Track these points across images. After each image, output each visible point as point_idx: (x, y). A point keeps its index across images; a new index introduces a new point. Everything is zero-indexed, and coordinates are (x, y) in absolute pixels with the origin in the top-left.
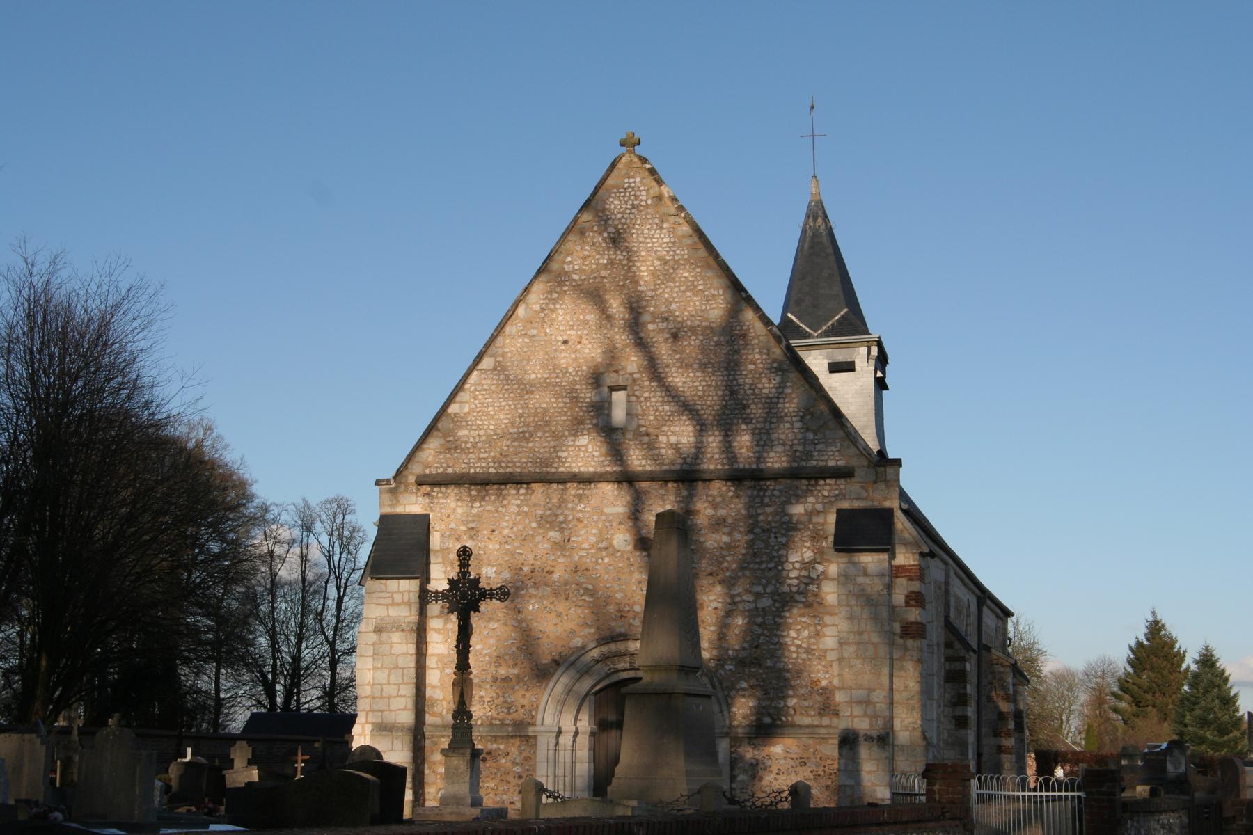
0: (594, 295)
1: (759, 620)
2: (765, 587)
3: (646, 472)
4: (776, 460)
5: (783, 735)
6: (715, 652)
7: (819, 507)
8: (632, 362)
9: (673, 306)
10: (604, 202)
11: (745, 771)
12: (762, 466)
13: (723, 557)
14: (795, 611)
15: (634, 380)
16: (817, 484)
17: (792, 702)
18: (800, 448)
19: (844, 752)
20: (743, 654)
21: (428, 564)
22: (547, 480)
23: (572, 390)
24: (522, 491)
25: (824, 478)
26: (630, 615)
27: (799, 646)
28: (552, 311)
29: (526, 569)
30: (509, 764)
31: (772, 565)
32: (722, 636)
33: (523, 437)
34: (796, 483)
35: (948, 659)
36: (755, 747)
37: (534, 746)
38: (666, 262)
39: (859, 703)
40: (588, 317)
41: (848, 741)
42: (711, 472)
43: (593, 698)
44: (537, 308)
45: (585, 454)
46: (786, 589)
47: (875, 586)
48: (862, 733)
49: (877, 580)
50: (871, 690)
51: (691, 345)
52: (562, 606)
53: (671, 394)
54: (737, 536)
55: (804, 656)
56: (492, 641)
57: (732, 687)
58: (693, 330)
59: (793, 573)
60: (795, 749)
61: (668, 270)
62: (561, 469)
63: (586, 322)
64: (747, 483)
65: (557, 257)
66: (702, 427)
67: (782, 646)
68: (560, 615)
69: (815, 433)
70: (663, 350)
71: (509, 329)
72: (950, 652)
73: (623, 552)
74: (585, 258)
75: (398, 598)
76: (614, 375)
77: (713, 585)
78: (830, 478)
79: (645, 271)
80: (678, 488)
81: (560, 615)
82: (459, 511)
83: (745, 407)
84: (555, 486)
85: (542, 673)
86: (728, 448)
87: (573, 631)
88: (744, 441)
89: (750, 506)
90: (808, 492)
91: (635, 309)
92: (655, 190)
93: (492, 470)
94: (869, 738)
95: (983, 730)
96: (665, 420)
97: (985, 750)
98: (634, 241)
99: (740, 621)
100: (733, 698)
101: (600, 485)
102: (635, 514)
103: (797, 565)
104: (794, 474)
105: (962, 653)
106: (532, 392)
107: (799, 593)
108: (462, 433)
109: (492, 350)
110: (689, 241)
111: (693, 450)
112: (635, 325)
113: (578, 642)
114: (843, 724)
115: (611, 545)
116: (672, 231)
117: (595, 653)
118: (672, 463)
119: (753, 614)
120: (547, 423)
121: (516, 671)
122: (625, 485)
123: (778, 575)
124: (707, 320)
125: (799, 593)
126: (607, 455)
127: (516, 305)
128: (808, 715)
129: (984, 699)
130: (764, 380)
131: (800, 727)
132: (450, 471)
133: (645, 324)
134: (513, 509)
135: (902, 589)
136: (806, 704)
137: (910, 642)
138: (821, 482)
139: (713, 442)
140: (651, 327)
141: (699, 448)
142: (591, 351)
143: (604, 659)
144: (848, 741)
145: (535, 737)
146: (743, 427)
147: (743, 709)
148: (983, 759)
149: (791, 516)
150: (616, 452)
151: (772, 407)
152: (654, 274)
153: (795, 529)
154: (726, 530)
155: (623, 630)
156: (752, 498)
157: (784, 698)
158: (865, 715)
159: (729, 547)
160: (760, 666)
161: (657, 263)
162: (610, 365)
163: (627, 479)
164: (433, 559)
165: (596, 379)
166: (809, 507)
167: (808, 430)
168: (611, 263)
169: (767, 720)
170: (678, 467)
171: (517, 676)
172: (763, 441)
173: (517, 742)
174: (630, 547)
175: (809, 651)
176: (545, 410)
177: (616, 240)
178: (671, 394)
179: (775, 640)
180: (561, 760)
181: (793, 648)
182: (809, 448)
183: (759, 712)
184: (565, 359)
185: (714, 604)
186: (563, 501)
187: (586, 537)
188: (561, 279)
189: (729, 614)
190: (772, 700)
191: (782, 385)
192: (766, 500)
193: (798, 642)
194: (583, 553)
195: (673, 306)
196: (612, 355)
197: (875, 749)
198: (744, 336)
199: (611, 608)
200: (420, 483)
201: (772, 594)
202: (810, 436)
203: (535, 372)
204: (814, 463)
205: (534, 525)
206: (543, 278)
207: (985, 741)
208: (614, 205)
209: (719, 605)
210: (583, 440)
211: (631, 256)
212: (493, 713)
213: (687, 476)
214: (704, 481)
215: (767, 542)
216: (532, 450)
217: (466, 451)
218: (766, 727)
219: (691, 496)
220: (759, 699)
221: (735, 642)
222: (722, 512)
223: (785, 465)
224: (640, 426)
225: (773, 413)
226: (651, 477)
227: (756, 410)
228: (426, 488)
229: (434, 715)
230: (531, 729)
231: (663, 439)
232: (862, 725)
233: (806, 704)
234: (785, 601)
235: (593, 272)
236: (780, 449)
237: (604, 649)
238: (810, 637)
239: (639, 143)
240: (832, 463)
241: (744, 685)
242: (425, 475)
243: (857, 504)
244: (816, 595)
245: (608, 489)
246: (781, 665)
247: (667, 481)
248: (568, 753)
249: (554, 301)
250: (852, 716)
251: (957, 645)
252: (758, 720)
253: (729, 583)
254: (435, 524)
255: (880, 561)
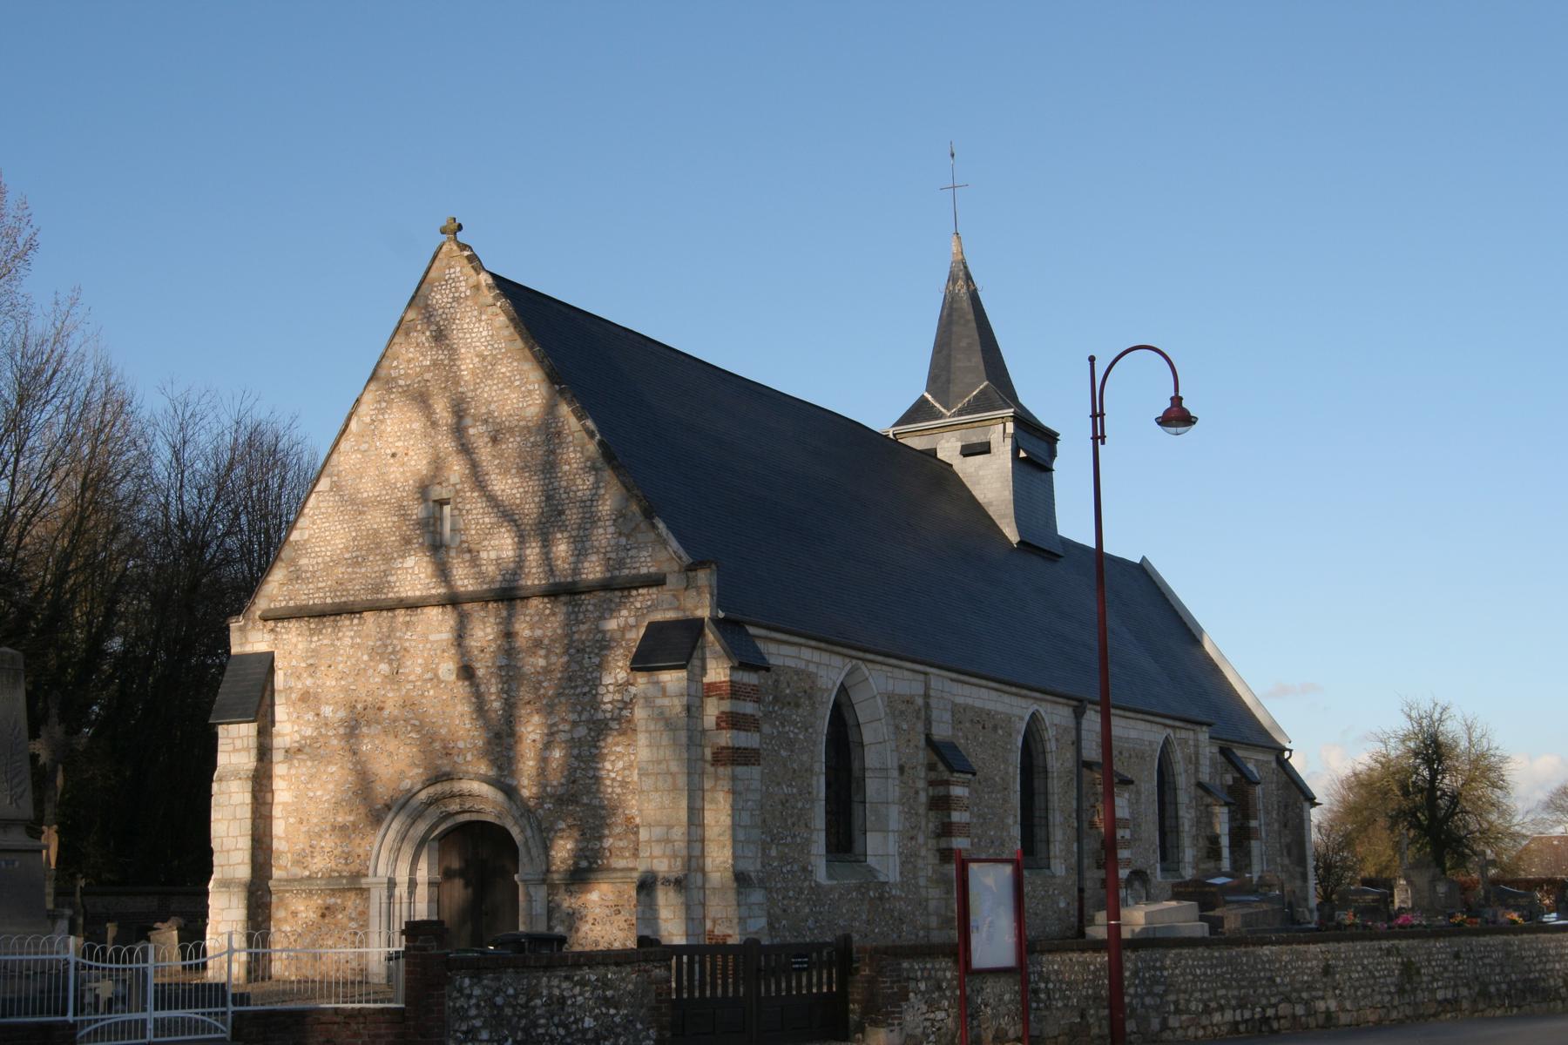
0: (421, 399)
1: (576, 752)
2: (580, 714)
3: (467, 593)
4: (593, 570)
5: (597, 881)
6: (534, 790)
7: (632, 621)
8: (456, 469)
9: (493, 407)
10: (427, 298)
11: (563, 922)
12: (577, 578)
13: (540, 682)
14: (610, 740)
15: (457, 492)
16: (630, 595)
17: (608, 843)
18: (613, 555)
19: (642, 897)
20: (561, 791)
21: (272, 705)
22: (377, 607)
23: (401, 507)
24: (356, 621)
25: (636, 588)
26: (455, 751)
27: (614, 780)
28: (382, 422)
29: (359, 706)
30: (345, 920)
31: (586, 689)
32: (542, 772)
33: (356, 562)
34: (609, 595)
35: (931, 783)
36: (571, 893)
37: (368, 899)
38: (484, 358)
39: (658, 841)
40: (416, 426)
41: (647, 886)
42: (528, 587)
43: (436, 845)
44: (368, 420)
45: (414, 575)
46: (600, 716)
47: (676, 706)
48: (661, 876)
49: (676, 701)
50: (670, 827)
51: (511, 445)
52: (392, 745)
53: (492, 500)
54: (553, 659)
55: (618, 790)
56: (331, 786)
57: (551, 829)
58: (511, 430)
59: (609, 697)
60: (611, 896)
61: (488, 364)
62: (391, 595)
63: (412, 431)
64: (563, 599)
65: (386, 363)
66: (522, 540)
67: (598, 780)
68: (391, 754)
69: (628, 537)
70: (485, 453)
71: (343, 446)
72: (933, 775)
73: (447, 683)
74: (409, 361)
75: (238, 744)
76: (438, 488)
77: (530, 714)
78: (642, 587)
79: (467, 366)
80: (498, 609)
81: (391, 754)
82: (300, 646)
83: (561, 513)
84: (384, 613)
85: (377, 816)
86: (547, 560)
87: (402, 772)
88: (562, 549)
89: (567, 625)
90: (621, 605)
91: (459, 411)
92: (473, 279)
93: (329, 601)
94: (666, 882)
95: (1086, 861)
96: (488, 533)
97: (1088, 884)
98: (456, 336)
99: (557, 754)
100: (552, 840)
101: (427, 610)
102: (460, 636)
103: (611, 688)
104: (606, 586)
105: (946, 775)
106: (364, 513)
107: (612, 719)
108: (303, 561)
109: (329, 469)
110: (506, 333)
111: (512, 565)
112: (459, 431)
113: (407, 784)
114: (642, 866)
115: (436, 675)
116: (490, 323)
117: (423, 796)
118: (493, 581)
119: (573, 743)
120: (378, 546)
121: (352, 818)
122: (449, 608)
123: (595, 703)
124: (524, 419)
125: (612, 719)
126: (433, 576)
127: (349, 419)
128: (623, 857)
129: (1086, 825)
130: (579, 482)
131: (615, 870)
132: (292, 604)
133: (466, 428)
134: (348, 641)
135: (712, 710)
136: (621, 844)
137: (721, 770)
138: (634, 593)
139: (533, 552)
140: (471, 431)
141: (520, 561)
142: (418, 463)
143: (433, 802)
144: (647, 886)
145: (368, 890)
146: (559, 536)
147: (563, 849)
148: (1086, 895)
149: (604, 632)
150: (443, 572)
151: (588, 507)
152: (473, 373)
153: (608, 647)
154: (542, 652)
155: (447, 769)
156: (568, 614)
157: (601, 838)
158: (664, 855)
159: (547, 671)
160: (577, 803)
161: (476, 360)
162: (435, 476)
163: (453, 601)
164: (278, 700)
165: (423, 490)
166: (622, 621)
167: (620, 534)
168: (435, 363)
169: (584, 864)
170: (497, 585)
171: (354, 824)
172: (581, 549)
173: (352, 895)
174: (453, 677)
175: (624, 784)
176: (376, 531)
177: (440, 337)
178: (492, 500)
179: (591, 773)
180: (397, 913)
181: (608, 782)
182: (622, 554)
183: (579, 854)
184: (395, 473)
185: (533, 736)
186: (392, 630)
187: (414, 667)
188: (389, 384)
189: (548, 746)
190: (588, 841)
191: (596, 486)
192: (581, 616)
193: (613, 775)
194: (410, 686)
195: (493, 407)
196: (437, 465)
197: (672, 894)
198: (559, 433)
199: (437, 745)
200: (265, 619)
201: (588, 721)
202: (623, 541)
203: (368, 488)
204: (626, 572)
205: (366, 658)
206: (372, 386)
207: (1088, 874)
208: (439, 298)
209: (537, 737)
210: (410, 562)
211: (453, 352)
212: (333, 864)
213: (507, 595)
214: (523, 598)
215: (580, 663)
216: (365, 576)
217: (306, 581)
218: (582, 874)
219: (510, 616)
220: (577, 841)
221: (556, 779)
222: (538, 633)
223: (599, 575)
224: (462, 542)
225: (590, 519)
226: (475, 598)
227: (572, 515)
228: (271, 624)
229: (280, 868)
230: (363, 880)
231: (484, 555)
232: (662, 866)
233: (621, 844)
234: (599, 729)
235: (417, 375)
236: (594, 558)
237: (431, 790)
238: (624, 769)
239: (460, 227)
240: (644, 571)
241: (562, 825)
242: (270, 610)
243: (671, 615)
244: (629, 721)
245: (434, 613)
246: (596, 802)
247: (487, 602)
248: (405, 906)
249: (382, 411)
250: (652, 857)
251: (941, 767)
252: (576, 864)
253: (549, 709)
254: (278, 663)
255: (679, 680)
